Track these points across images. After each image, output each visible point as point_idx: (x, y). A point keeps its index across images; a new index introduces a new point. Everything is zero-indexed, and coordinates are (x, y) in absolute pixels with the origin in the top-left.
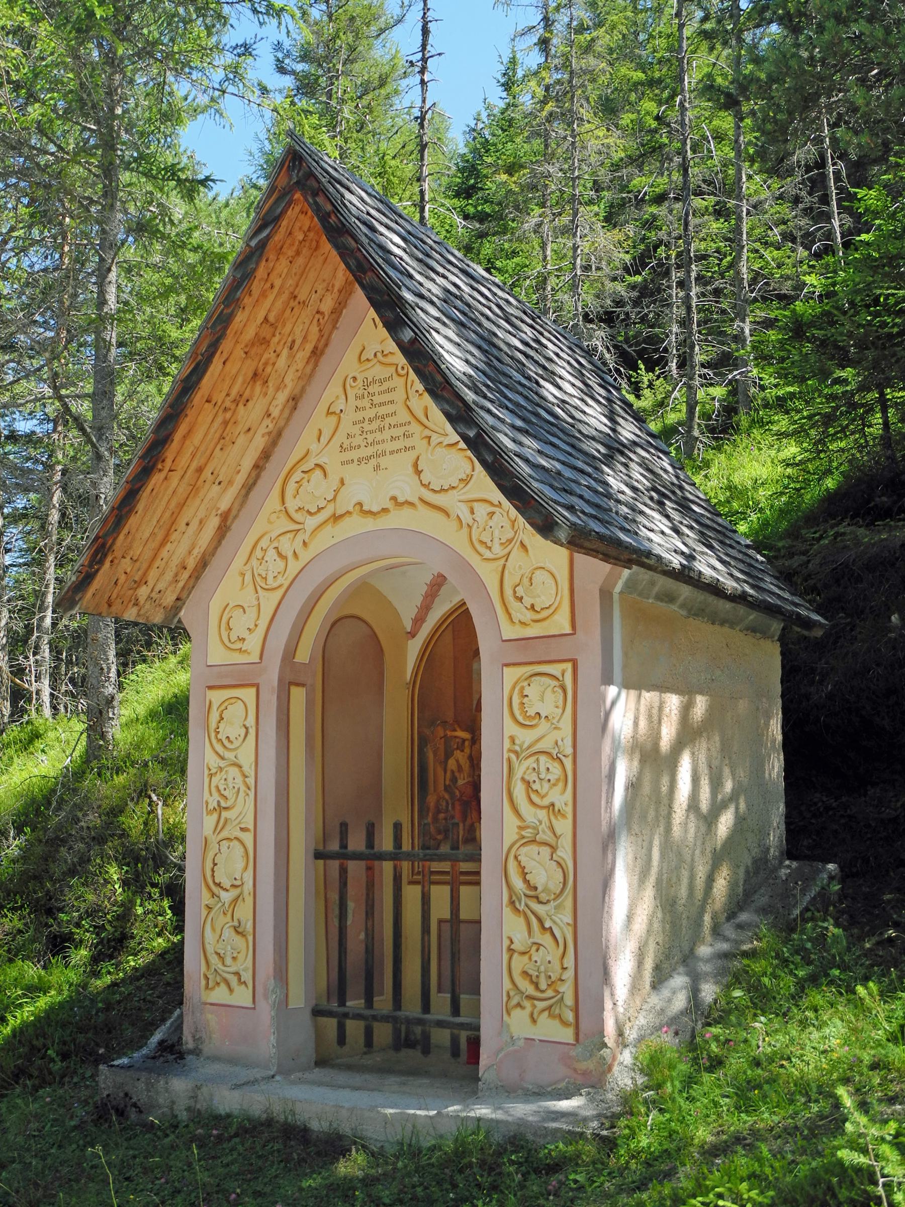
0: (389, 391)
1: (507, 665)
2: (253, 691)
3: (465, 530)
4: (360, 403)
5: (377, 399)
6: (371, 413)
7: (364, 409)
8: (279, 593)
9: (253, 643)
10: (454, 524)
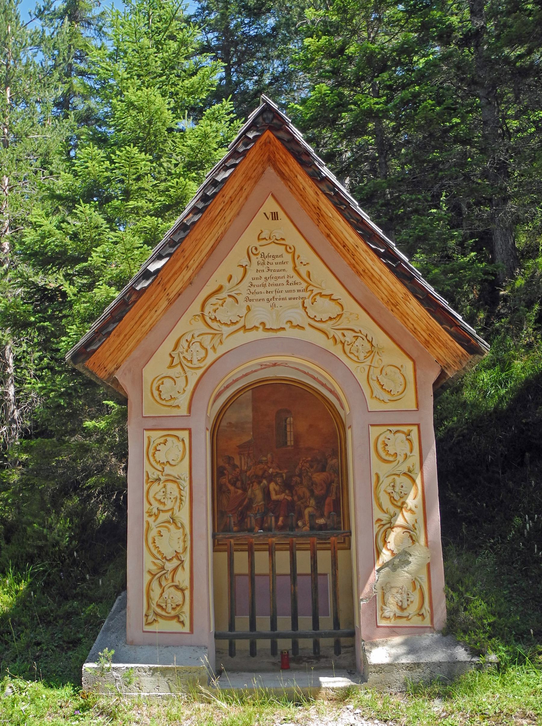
3: (340, 346)
8: (201, 371)
9: (183, 400)
10: (331, 341)
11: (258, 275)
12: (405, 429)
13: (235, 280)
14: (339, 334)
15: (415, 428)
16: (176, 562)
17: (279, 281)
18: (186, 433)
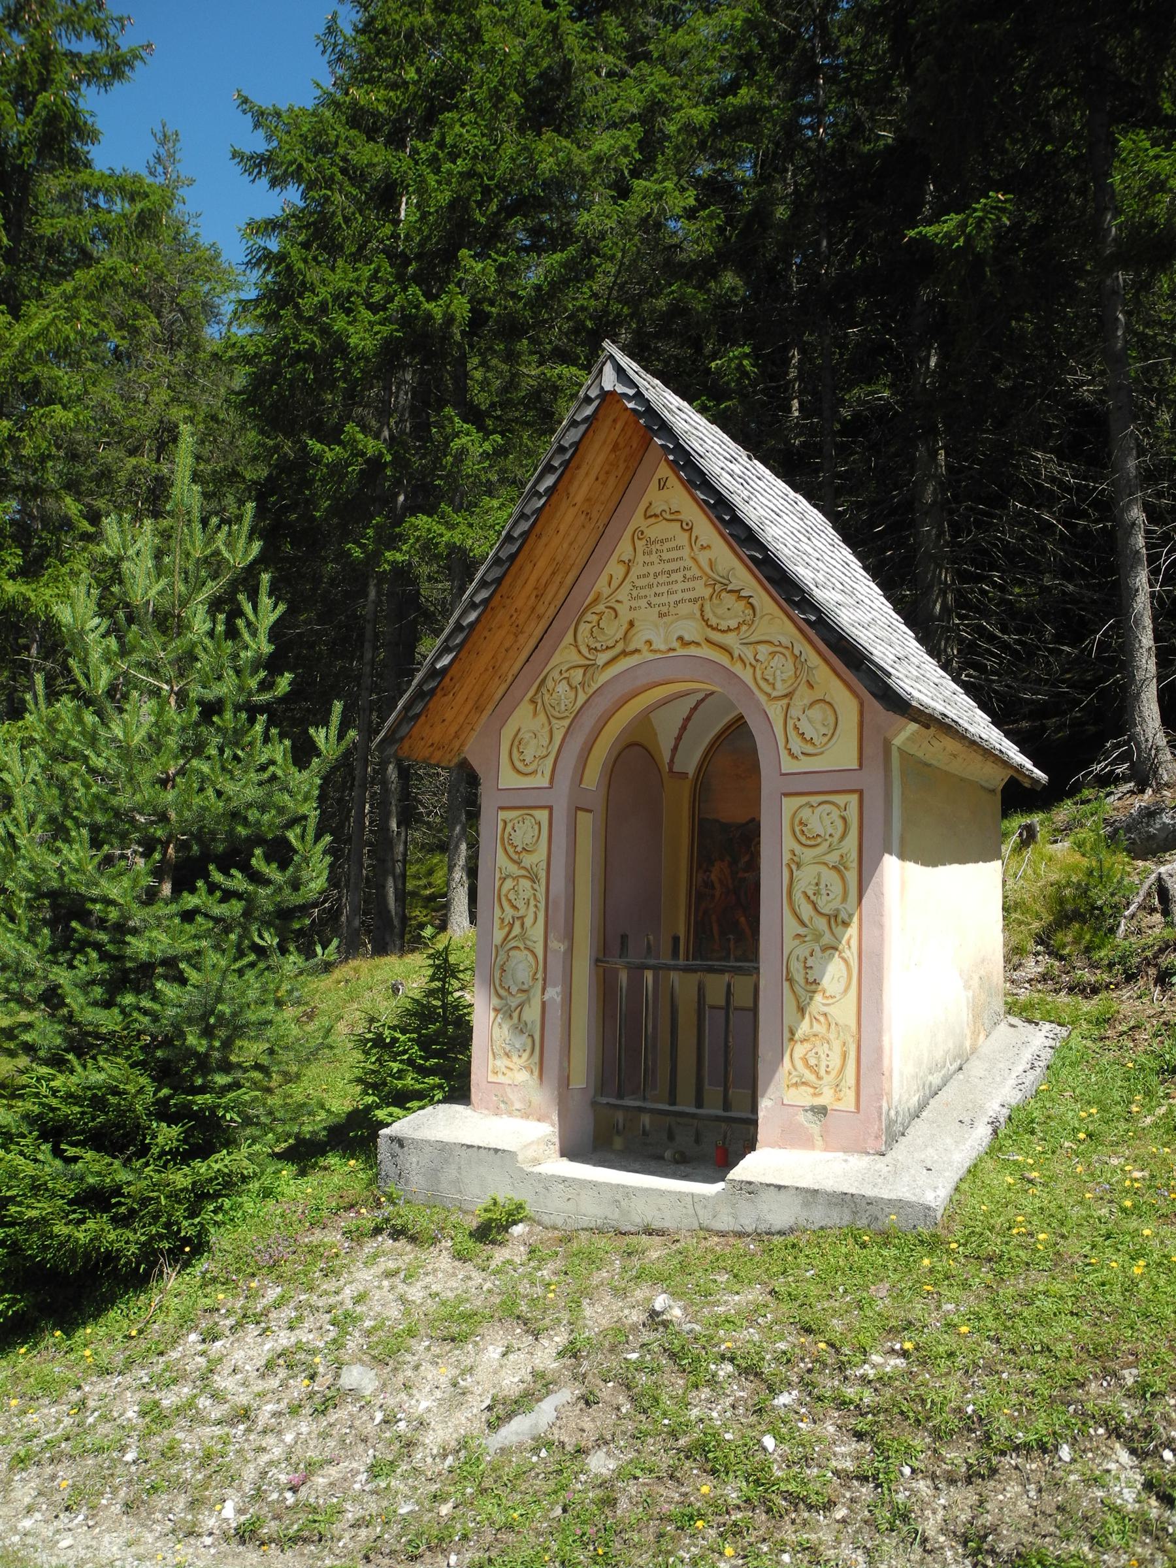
0: (678, 548)
1: (786, 795)
2: (546, 813)
4: (647, 559)
5: (666, 556)
6: (658, 568)
7: (652, 563)
8: (566, 723)
11: (645, 570)
12: (840, 799)
13: (615, 584)
14: (748, 654)
15: (854, 799)
16: (521, 997)
17: (674, 577)
18: (546, 813)
